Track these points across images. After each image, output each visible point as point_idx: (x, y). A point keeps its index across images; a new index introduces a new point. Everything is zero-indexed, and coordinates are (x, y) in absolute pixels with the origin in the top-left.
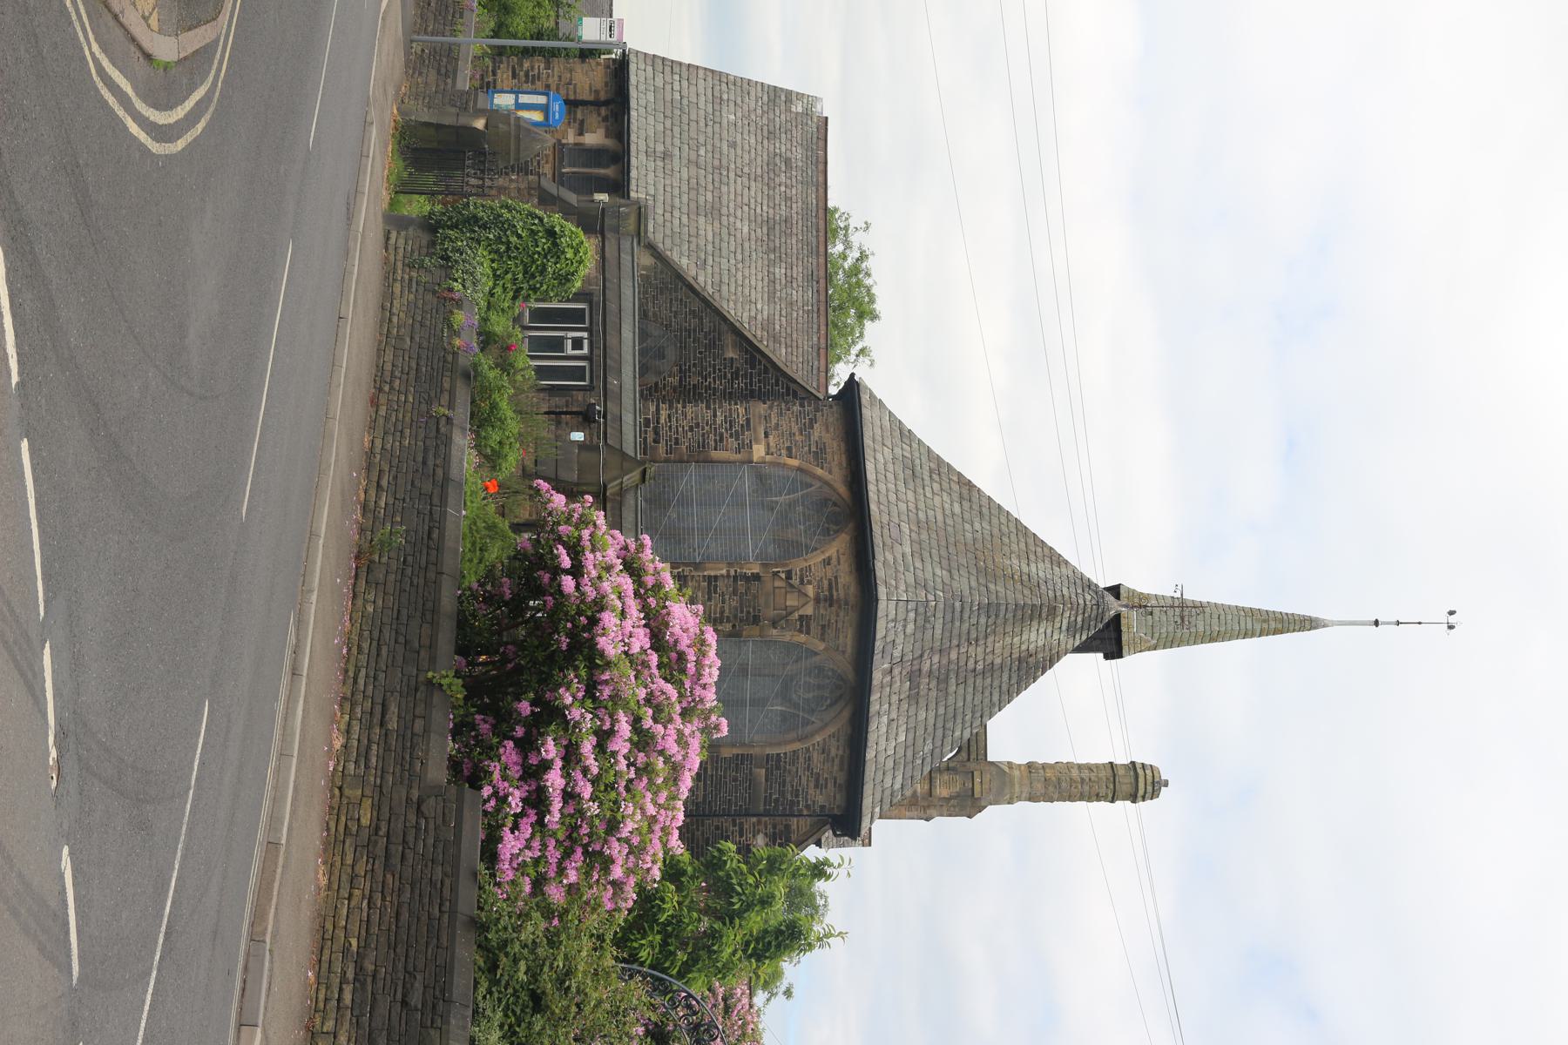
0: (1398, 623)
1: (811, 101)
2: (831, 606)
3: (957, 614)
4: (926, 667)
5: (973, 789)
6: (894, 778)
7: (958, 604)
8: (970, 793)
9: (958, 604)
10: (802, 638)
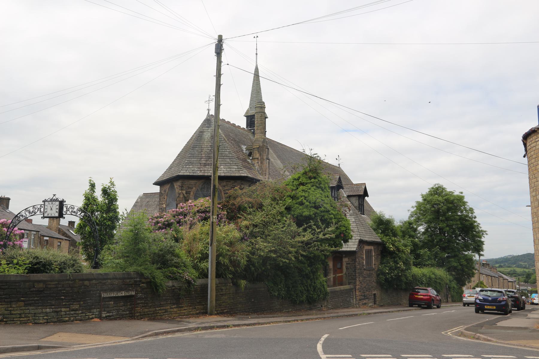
0: (257, 49)
1: (140, 198)
2: (183, 186)
3: (192, 155)
4: (204, 162)
5: (257, 148)
6: (233, 168)
7: (189, 155)
8: (258, 149)
9: (189, 155)
10: (192, 193)
